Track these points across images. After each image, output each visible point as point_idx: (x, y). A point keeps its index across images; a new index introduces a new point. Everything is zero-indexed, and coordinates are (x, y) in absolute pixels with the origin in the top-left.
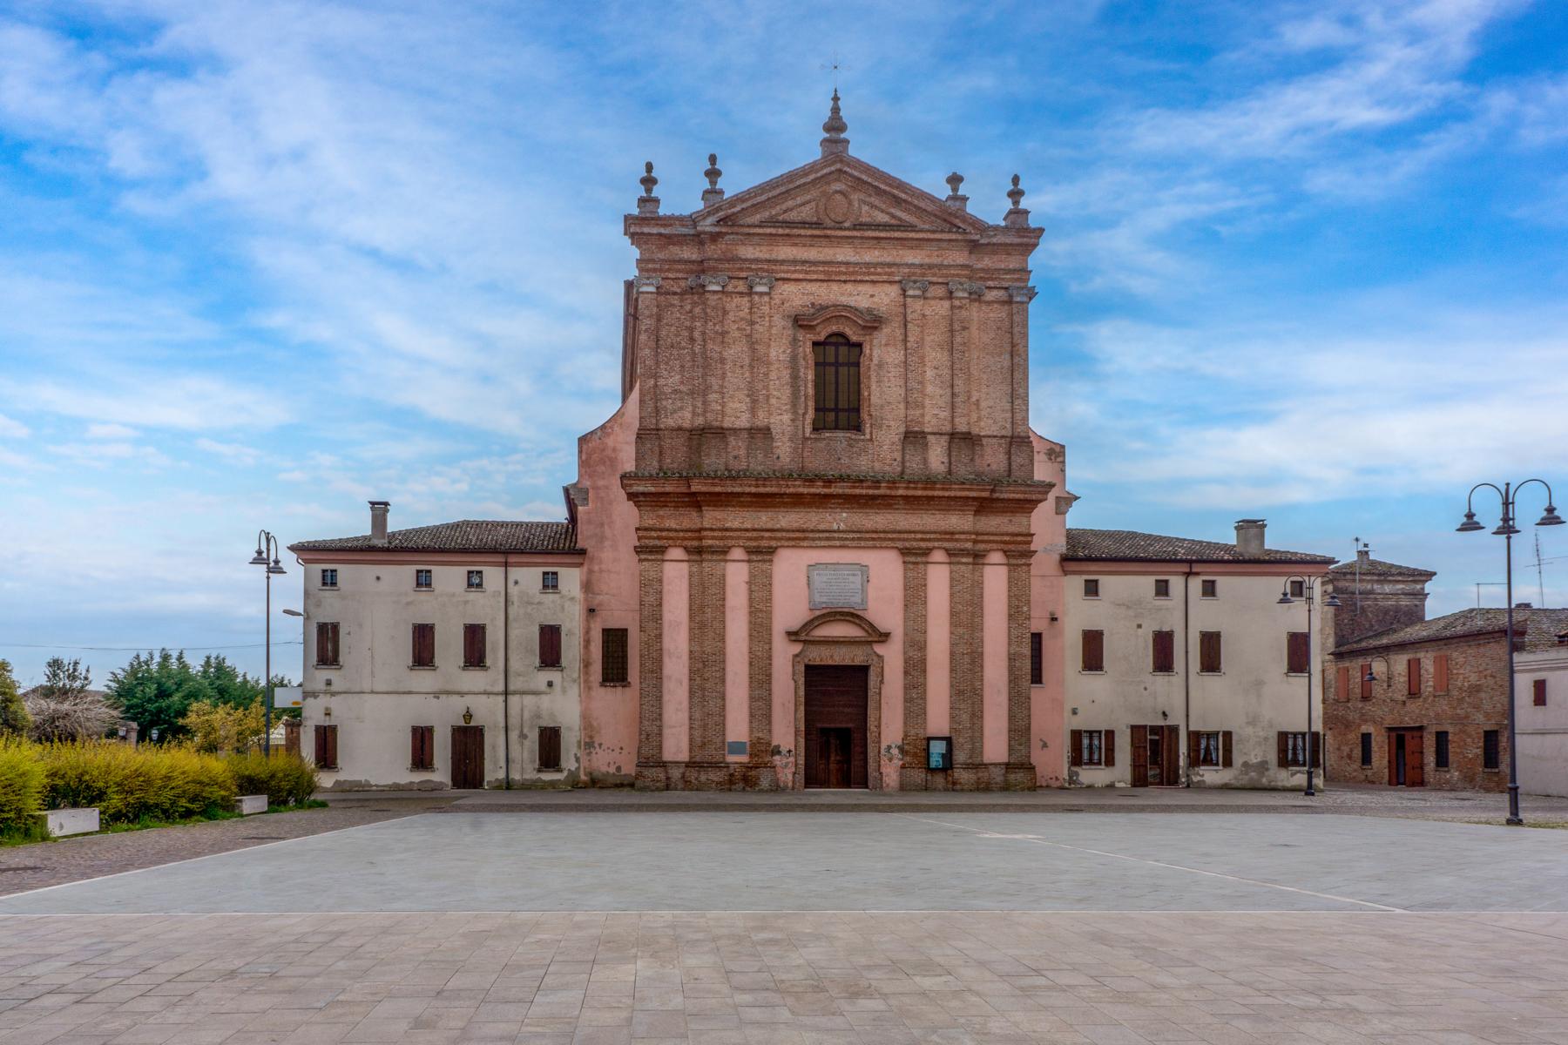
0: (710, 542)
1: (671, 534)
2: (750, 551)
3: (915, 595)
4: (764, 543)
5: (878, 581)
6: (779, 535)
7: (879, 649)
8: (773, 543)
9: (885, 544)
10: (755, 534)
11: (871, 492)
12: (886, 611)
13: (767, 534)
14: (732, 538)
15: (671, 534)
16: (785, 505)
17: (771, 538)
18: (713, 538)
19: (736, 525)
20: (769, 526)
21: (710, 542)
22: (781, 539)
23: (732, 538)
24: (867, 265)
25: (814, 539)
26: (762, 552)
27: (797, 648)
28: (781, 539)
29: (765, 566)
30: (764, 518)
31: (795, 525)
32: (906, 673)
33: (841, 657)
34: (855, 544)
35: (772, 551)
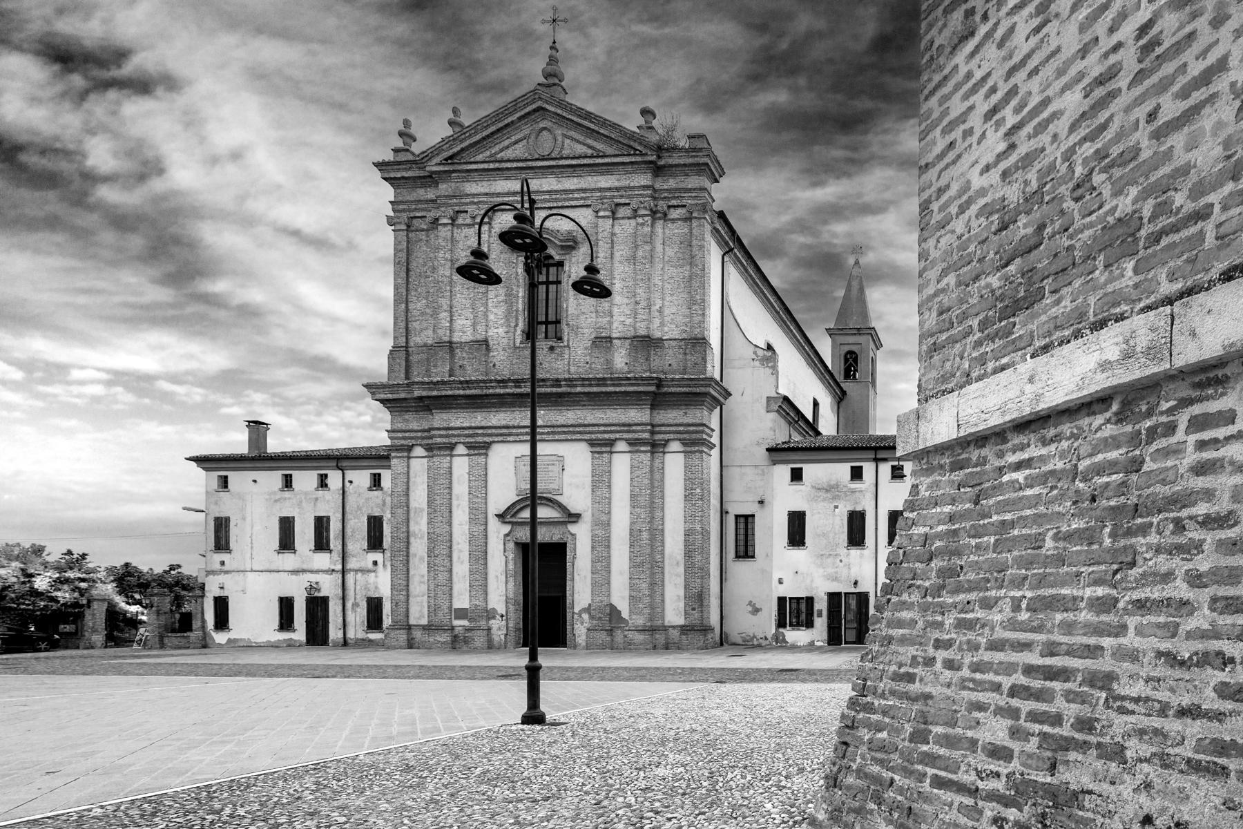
0: (439, 440)
1: (412, 435)
2: (470, 446)
3: (601, 481)
4: (480, 439)
5: (571, 470)
6: (489, 431)
7: (572, 528)
8: (487, 439)
9: (574, 437)
10: (471, 432)
11: (554, 390)
12: (577, 496)
13: (480, 431)
14: (455, 436)
15: (412, 435)
16: (493, 406)
17: (484, 435)
18: (441, 436)
19: (458, 424)
20: (483, 424)
21: (439, 440)
22: (491, 435)
23: (455, 436)
24: (566, 191)
25: (518, 435)
26: (480, 448)
27: (507, 529)
28: (491, 435)
29: (482, 459)
30: (480, 418)
31: (503, 423)
32: (593, 548)
33: (544, 535)
34: (550, 437)
35: (487, 446)
